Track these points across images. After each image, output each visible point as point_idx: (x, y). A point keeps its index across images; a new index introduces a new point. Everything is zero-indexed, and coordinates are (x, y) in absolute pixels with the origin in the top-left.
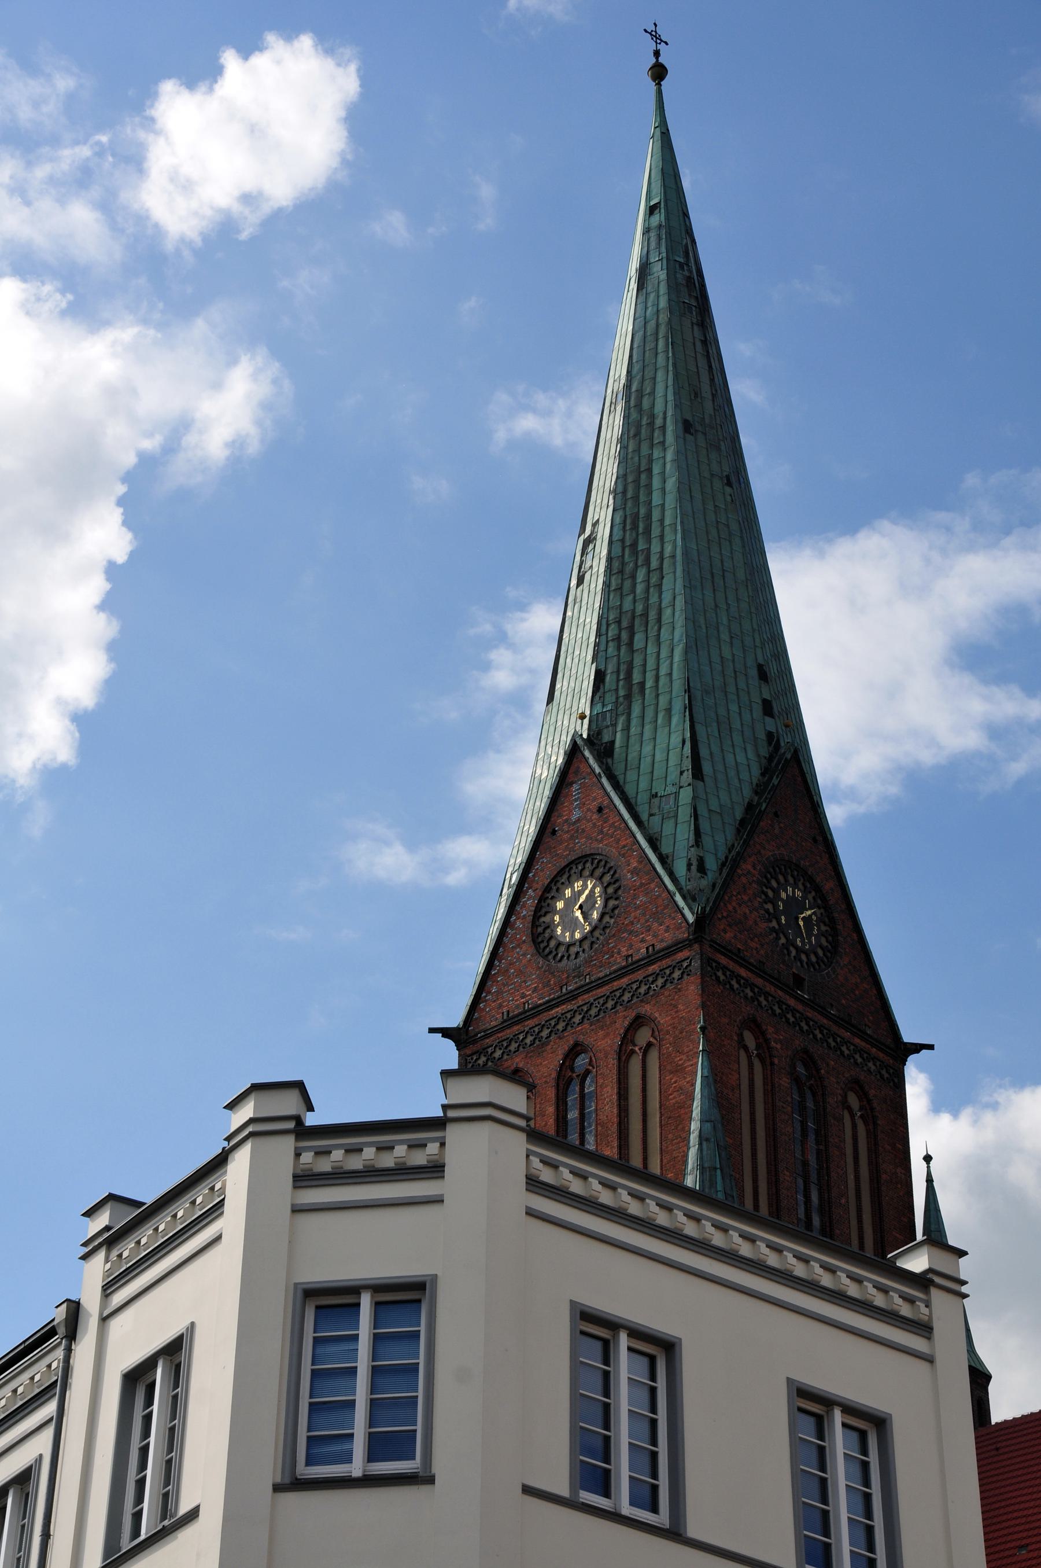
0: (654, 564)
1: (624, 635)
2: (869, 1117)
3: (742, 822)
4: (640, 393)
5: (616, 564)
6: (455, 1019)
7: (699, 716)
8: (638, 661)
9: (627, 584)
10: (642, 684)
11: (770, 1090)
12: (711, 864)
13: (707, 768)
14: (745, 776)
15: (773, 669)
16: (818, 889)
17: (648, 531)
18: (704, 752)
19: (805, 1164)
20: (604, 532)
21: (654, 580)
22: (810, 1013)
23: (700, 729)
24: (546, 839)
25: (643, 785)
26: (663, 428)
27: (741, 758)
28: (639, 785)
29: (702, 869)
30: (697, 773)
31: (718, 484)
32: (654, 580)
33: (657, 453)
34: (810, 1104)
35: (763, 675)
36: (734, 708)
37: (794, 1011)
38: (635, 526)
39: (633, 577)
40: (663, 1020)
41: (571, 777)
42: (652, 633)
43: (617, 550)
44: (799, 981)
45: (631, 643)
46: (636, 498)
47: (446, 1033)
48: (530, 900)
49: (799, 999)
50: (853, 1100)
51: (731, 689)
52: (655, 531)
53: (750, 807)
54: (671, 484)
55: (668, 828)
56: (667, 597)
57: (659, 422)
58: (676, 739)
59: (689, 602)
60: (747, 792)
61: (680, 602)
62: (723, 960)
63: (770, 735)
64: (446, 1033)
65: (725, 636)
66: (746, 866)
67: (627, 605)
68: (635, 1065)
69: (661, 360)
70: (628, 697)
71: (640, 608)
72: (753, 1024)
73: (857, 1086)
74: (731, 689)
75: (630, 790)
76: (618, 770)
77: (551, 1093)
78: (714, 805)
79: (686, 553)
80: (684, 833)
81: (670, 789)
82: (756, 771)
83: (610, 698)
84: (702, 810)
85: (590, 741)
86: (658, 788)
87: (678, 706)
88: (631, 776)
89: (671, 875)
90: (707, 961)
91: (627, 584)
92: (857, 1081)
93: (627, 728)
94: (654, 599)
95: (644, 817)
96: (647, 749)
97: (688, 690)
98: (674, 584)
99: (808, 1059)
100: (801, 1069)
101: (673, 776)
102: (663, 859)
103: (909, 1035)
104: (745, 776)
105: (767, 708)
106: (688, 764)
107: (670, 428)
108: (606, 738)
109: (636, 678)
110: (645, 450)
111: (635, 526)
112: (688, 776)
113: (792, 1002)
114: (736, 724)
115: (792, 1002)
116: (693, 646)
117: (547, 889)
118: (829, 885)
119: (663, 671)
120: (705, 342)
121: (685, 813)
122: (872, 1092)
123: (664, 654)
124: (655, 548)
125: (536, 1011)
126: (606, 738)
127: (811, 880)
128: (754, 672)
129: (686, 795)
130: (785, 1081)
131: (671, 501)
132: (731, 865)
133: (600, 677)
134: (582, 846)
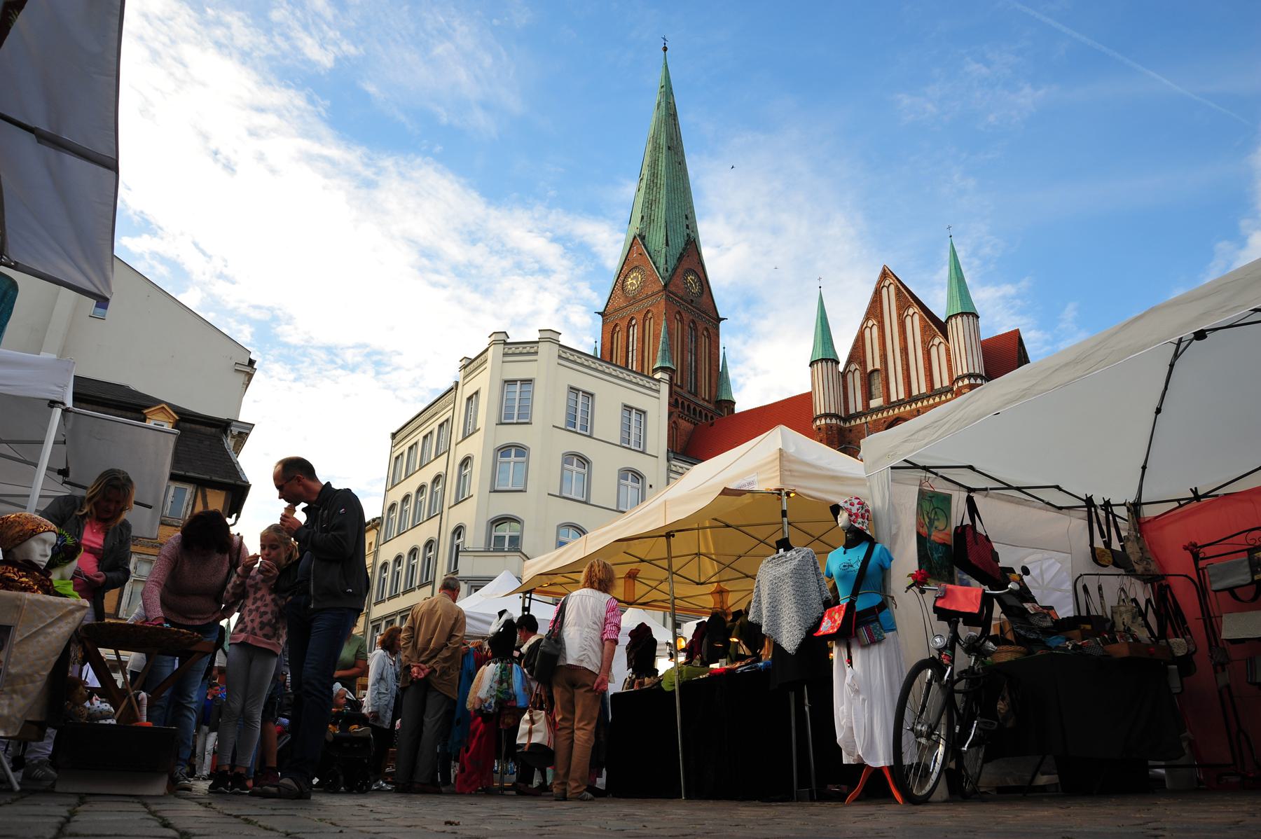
1: (650, 206)
2: (709, 337)
4: (656, 138)
5: (648, 186)
7: (669, 229)
8: (653, 213)
9: (651, 192)
10: (654, 220)
11: (683, 329)
12: (670, 270)
13: (670, 243)
14: (680, 245)
15: (689, 216)
16: (699, 276)
17: (657, 177)
18: (669, 239)
19: (691, 349)
20: (645, 177)
22: (694, 310)
26: (662, 148)
27: (679, 241)
28: (652, 247)
29: (667, 271)
30: (667, 244)
31: (677, 164)
33: (660, 155)
34: (693, 333)
35: (687, 218)
36: (678, 226)
37: (690, 309)
38: (654, 176)
39: (653, 190)
41: (634, 245)
42: (657, 206)
43: (649, 182)
44: (692, 301)
46: (654, 168)
48: (622, 278)
49: (692, 306)
50: (705, 333)
51: (678, 221)
52: (659, 177)
53: (681, 254)
54: (664, 164)
56: (661, 196)
57: (661, 147)
58: (662, 235)
59: (668, 197)
60: (681, 250)
61: (665, 197)
62: (671, 295)
63: (688, 234)
65: (677, 207)
66: (679, 270)
68: (647, 322)
69: (663, 130)
70: (650, 223)
71: (654, 198)
72: (679, 313)
73: (707, 329)
74: (678, 221)
75: (649, 249)
76: (646, 244)
77: (626, 330)
78: (671, 253)
79: (667, 184)
80: (663, 261)
82: (683, 244)
83: (645, 223)
84: (668, 255)
85: (639, 235)
86: (657, 248)
87: (663, 225)
88: (650, 245)
89: (659, 272)
90: (667, 296)
91: (651, 192)
92: (707, 328)
94: (658, 196)
95: (652, 256)
96: (654, 238)
97: (666, 222)
98: (663, 192)
99: (693, 322)
100: (691, 325)
101: (661, 245)
102: (657, 268)
103: (721, 316)
104: (680, 245)
105: (687, 227)
106: (665, 242)
107: (664, 148)
109: (652, 218)
110: (657, 155)
111: (654, 176)
112: (664, 246)
113: (690, 307)
114: (679, 231)
115: (690, 307)
116: (668, 209)
117: (627, 275)
118: (702, 276)
120: (675, 124)
121: (663, 255)
122: (710, 331)
124: (659, 182)
125: (622, 308)
126: (643, 234)
127: (697, 274)
128: (684, 217)
129: (664, 251)
130: (687, 327)
131: (664, 169)
132: (675, 270)
133: (643, 217)
134: (636, 263)
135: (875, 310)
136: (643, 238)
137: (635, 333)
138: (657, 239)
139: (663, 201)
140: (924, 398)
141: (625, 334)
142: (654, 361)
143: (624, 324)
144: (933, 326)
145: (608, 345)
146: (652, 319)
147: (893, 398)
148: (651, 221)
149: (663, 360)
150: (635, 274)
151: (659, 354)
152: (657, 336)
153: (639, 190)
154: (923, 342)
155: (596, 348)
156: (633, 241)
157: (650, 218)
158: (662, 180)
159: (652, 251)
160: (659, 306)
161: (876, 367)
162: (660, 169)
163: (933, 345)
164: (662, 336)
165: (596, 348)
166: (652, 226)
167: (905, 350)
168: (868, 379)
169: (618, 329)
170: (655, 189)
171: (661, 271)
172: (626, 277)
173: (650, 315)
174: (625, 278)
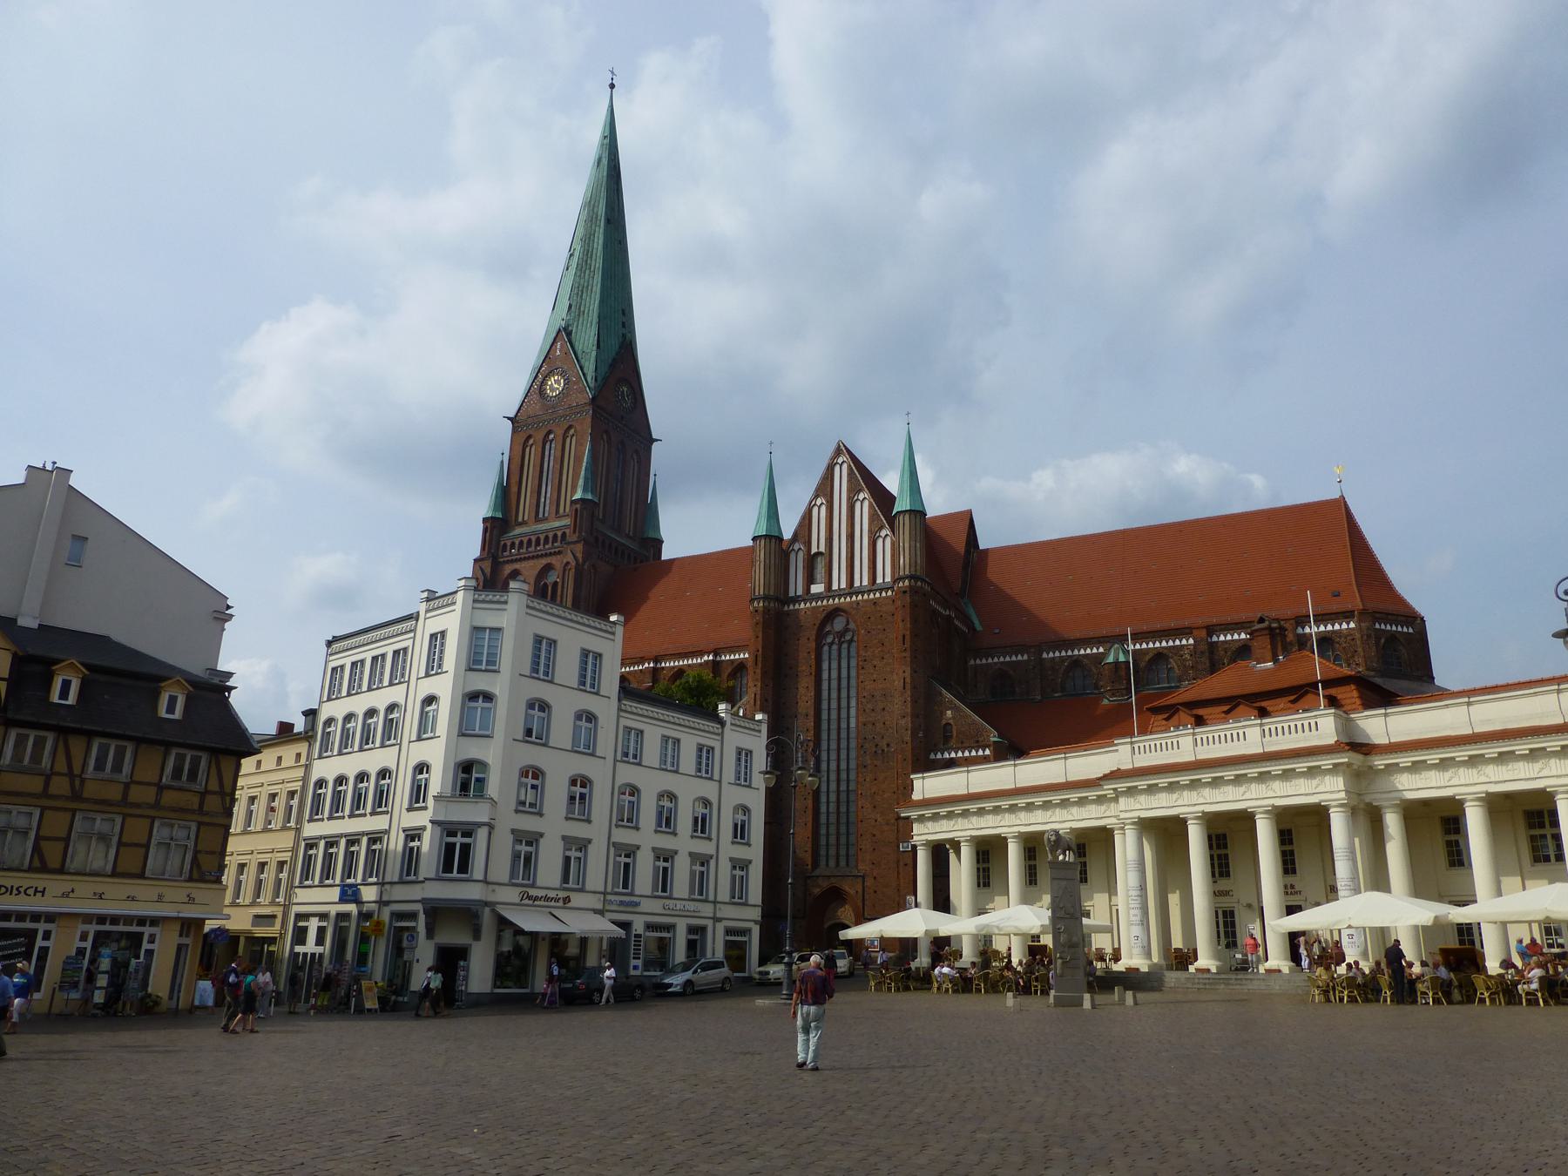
0: (592, 269)
3: (611, 365)
6: (512, 415)
12: (599, 379)
13: (601, 344)
18: (601, 339)
21: (591, 275)
23: (601, 331)
24: (547, 359)
25: (581, 346)
28: (579, 347)
30: (598, 347)
32: (591, 275)
35: (624, 314)
40: (578, 428)
42: (589, 294)
45: (582, 296)
47: (509, 418)
55: (587, 364)
58: (592, 333)
59: (602, 285)
64: (509, 418)
67: (582, 283)
68: (568, 440)
70: (579, 315)
71: (586, 284)
75: (576, 348)
77: (541, 445)
81: (589, 351)
85: (565, 329)
93: (577, 327)
94: (591, 282)
95: (580, 358)
98: (598, 278)
102: (584, 374)
106: (596, 342)
108: (570, 328)
109: (582, 309)
112: (595, 348)
119: (591, 308)
123: (592, 302)
129: (594, 353)
133: (570, 306)
135: (825, 487)
136: (569, 334)
137: (553, 450)
138: (587, 338)
139: (597, 289)
140: (864, 592)
141: (540, 449)
142: (574, 491)
143: (540, 436)
144: (882, 517)
145: (517, 460)
146: (574, 438)
147: (835, 587)
148: (580, 313)
149: (585, 490)
150: (556, 378)
151: (581, 482)
152: (578, 460)
153: (567, 269)
154: (870, 531)
155: (502, 462)
156: (557, 335)
157: (580, 308)
158: (598, 263)
159: (579, 353)
160: (585, 425)
161: (820, 550)
162: (595, 246)
163: (879, 536)
164: (585, 460)
165: (502, 462)
166: (581, 319)
167: (851, 537)
168: (811, 560)
169: (531, 441)
170: (587, 272)
171: (589, 379)
172: (543, 382)
173: (572, 431)
174: (544, 379)
